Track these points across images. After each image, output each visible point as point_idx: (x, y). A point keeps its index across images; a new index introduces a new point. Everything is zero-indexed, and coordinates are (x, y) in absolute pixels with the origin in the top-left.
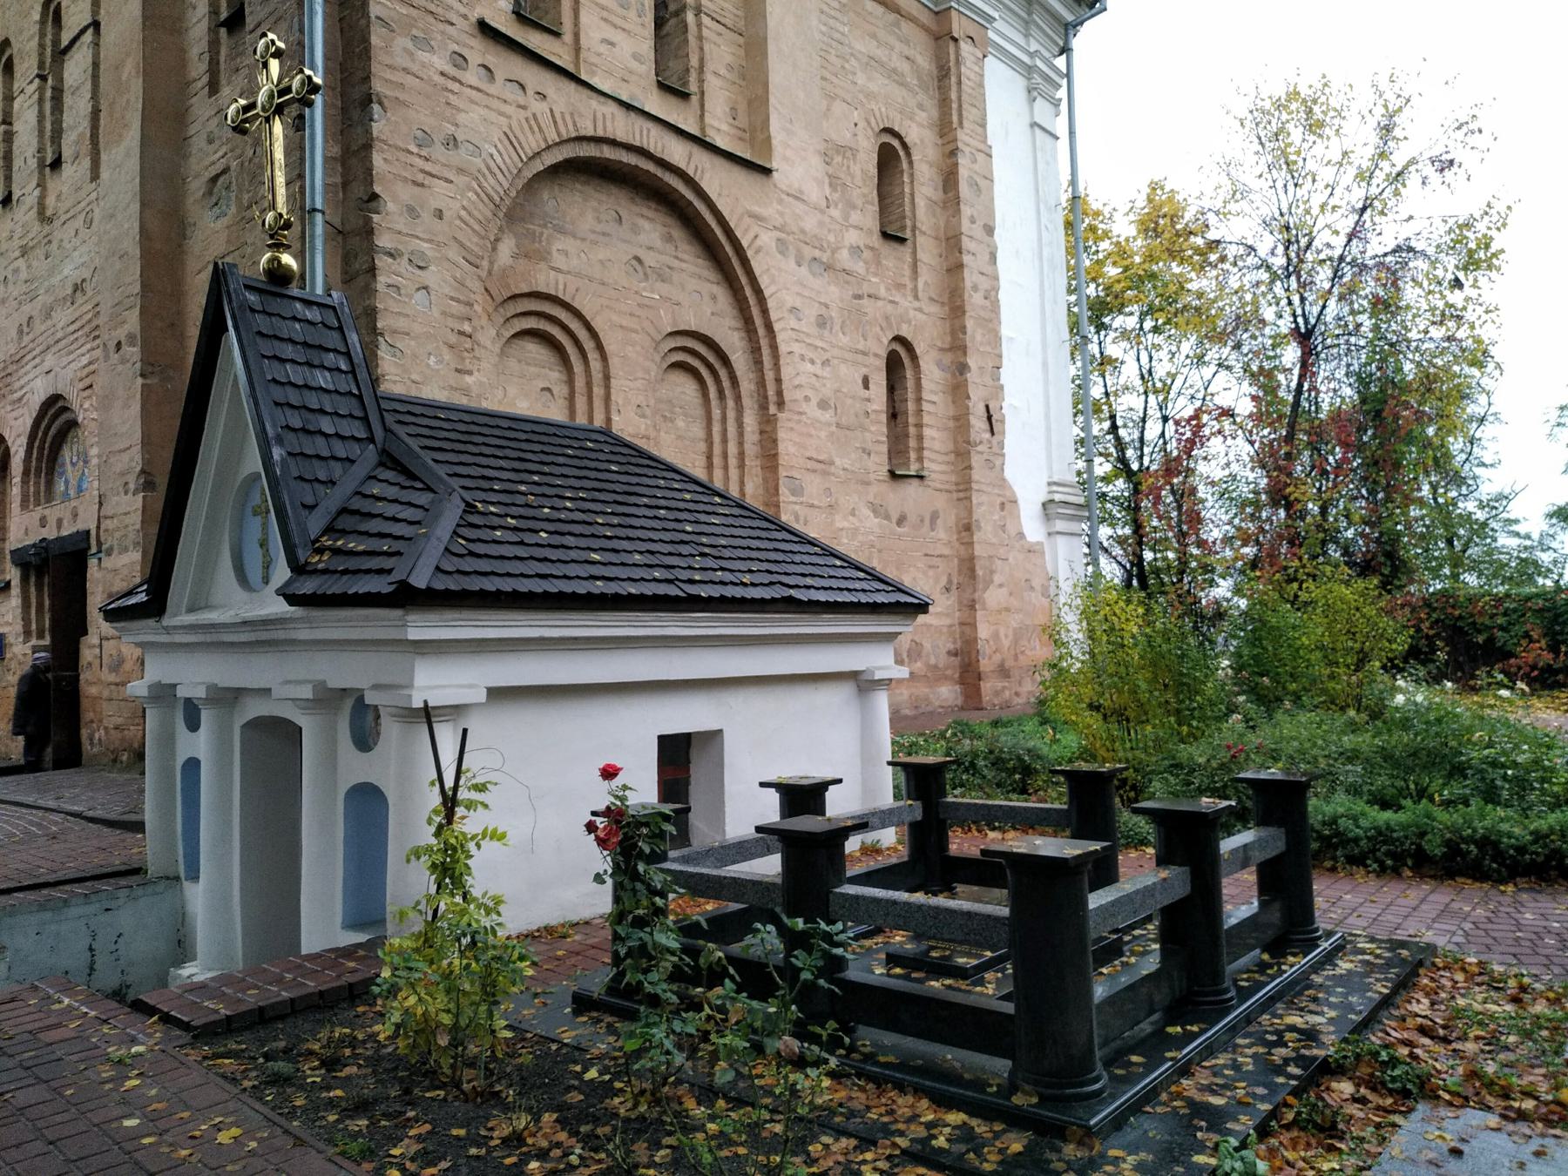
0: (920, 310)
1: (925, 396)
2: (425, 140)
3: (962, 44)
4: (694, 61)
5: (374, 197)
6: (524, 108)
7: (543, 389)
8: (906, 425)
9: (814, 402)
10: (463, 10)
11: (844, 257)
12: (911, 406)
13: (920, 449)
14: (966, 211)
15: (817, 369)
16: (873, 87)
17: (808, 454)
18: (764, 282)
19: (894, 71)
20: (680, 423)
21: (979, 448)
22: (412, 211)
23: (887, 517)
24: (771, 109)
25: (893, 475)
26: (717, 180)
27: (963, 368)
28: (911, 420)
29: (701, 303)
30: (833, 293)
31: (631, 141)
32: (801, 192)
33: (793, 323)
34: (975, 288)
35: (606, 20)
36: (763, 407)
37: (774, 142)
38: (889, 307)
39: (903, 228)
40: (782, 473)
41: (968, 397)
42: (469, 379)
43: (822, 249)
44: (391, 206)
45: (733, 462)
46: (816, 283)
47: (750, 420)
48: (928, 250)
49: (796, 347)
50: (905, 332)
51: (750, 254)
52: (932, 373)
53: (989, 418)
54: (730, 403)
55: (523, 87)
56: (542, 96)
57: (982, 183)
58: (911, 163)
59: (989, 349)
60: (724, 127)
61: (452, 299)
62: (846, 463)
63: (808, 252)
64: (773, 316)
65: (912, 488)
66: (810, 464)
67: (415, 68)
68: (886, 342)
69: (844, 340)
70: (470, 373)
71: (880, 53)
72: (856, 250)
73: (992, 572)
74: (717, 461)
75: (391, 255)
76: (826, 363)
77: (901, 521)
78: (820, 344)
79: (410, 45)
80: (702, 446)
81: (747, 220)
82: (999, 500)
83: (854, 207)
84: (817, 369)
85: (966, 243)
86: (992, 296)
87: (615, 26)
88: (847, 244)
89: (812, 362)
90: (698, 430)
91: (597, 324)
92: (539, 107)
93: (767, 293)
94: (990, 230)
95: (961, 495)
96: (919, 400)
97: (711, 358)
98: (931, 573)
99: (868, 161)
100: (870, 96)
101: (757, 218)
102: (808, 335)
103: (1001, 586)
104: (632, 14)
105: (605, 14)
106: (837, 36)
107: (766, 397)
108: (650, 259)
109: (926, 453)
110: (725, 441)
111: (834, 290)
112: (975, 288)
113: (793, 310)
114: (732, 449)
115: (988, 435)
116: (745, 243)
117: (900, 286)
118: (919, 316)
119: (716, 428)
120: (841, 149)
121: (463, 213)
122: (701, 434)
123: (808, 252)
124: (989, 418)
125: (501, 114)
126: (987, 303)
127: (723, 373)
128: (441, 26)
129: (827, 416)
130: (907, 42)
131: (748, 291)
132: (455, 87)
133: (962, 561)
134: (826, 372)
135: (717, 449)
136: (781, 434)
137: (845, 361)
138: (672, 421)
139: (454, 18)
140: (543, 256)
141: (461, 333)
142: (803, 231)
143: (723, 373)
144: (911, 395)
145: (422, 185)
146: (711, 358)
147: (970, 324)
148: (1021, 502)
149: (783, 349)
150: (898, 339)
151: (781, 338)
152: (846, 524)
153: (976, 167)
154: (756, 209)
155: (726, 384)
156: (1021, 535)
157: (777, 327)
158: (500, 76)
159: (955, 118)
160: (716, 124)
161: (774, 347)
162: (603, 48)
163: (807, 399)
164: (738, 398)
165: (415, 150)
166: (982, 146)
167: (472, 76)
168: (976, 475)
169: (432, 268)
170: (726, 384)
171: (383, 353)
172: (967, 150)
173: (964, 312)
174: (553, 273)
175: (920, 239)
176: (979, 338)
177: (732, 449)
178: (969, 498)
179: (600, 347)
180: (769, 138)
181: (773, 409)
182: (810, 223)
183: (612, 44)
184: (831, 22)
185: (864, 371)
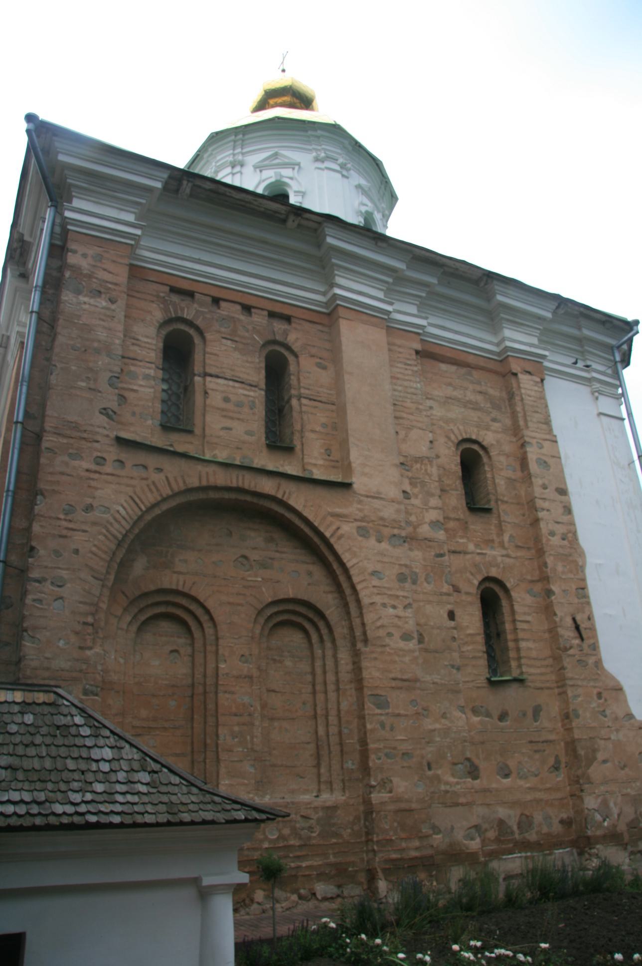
0: (508, 556)
1: (518, 617)
2: (70, 510)
3: (520, 376)
4: (298, 427)
5: (32, 549)
6: (146, 479)
7: (172, 651)
8: (506, 640)
9: (397, 634)
10: (105, 432)
11: (425, 530)
12: (508, 626)
13: (519, 658)
14: (537, 482)
15: (400, 612)
16: (451, 415)
17: (392, 675)
18: (345, 557)
19: (470, 402)
20: (288, 663)
21: (571, 652)
22: (57, 553)
23: (488, 715)
24: (351, 445)
25: (491, 683)
26: (300, 500)
27: (549, 593)
28: (510, 637)
30: (417, 557)
31: (229, 484)
32: (379, 493)
33: (375, 582)
34: (552, 534)
35: (225, 416)
36: (354, 644)
37: (353, 465)
38: (478, 558)
39: (489, 501)
40: (367, 692)
41: (555, 614)
42: (89, 653)
43: (400, 528)
44: (42, 552)
45: (331, 687)
46: (398, 552)
47: (344, 656)
48: (510, 515)
49: (378, 599)
50: (494, 572)
51: (332, 541)
52: (522, 603)
53: (577, 628)
54: (328, 645)
55: (145, 467)
56: (160, 470)
57: (551, 461)
58: (490, 457)
59: (571, 576)
60: (321, 462)
61: (81, 602)
62: (436, 678)
63: (387, 531)
64: (355, 579)
65: (512, 692)
66: (394, 684)
68: (476, 582)
69: (428, 587)
71: (457, 394)
72: (434, 524)
73: (595, 751)
74: (319, 687)
75: (39, 581)
76: (405, 607)
77: (503, 717)
78: (401, 593)
79: (66, 458)
80: (309, 678)
81: (330, 519)
82: (595, 691)
83: (432, 495)
84: (400, 612)
85: (539, 503)
86: (571, 537)
88: (427, 520)
89: (394, 607)
90: (305, 667)
91: (210, 604)
93: (349, 565)
94: (563, 492)
95: (560, 690)
96: (514, 621)
97: (311, 615)
98: (537, 756)
99: (452, 461)
100: (448, 421)
102: (389, 589)
103: (605, 762)
105: (225, 413)
106: (410, 390)
107: (354, 637)
108: (254, 556)
109: (523, 661)
110: (325, 672)
111: (417, 554)
112: (552, 534)
113: (374, 573)
114: (331, 677)
115: (577, 641)
116: (328, 534)
117: (489, 542)
118: (507, 560)
120: (419, 460)
121: (94, 549)
122: (308, 669)
123: (387, 531)
124: (577, 628)
125: (128, 485)
126: (565, 543)
127: (321, 625)
128: (89, 445)
129: (412, 645)
130: (479, 383)
131: (335, 566)
132: (96, 476)
133: (567, 744)
134: (409, 613)
135: (319, 678)
136: (365, 664)
137: (430, 602)
138: (281, 662)
139: (99, 438)
141: (85, 623)
142: (382, 519)
143: (321, 625)
144: (507, 618)
145: (65, 537)
146: (311, 615)
147: (550, 560)
148: (626, 689)
149: (365, 601)
150: (488, 579)
151: (362, 594)
152: (438, 726)
153: (544, 451)
154: (338, 510)
155: (324, 631)
156: (630, 716)
157: (359, 587)
158: (129, 464)
159: (521, 423)
160: (313, 461)
161: (358, 601)
162: (222, 433)
163: (389, 635)
164: (333, 641)
165: (62, 516)
166: (548, 437)
167: (108, 468)
168: (569, 674)
169: (69, 585)
170: (324, 631)
171: (27, 644)
172: (534, 441)
173: (544, 553)
174: (175, 576)
175: (502, 507)
176: (560, 568)
177: (331, 677)
178: (565, 693)
179: (212, 619)
180: (350, 464)
181: (360, 645)
182: (389, 512)
183: (230, 429)
184: (406, 383)
185: (449, 607)
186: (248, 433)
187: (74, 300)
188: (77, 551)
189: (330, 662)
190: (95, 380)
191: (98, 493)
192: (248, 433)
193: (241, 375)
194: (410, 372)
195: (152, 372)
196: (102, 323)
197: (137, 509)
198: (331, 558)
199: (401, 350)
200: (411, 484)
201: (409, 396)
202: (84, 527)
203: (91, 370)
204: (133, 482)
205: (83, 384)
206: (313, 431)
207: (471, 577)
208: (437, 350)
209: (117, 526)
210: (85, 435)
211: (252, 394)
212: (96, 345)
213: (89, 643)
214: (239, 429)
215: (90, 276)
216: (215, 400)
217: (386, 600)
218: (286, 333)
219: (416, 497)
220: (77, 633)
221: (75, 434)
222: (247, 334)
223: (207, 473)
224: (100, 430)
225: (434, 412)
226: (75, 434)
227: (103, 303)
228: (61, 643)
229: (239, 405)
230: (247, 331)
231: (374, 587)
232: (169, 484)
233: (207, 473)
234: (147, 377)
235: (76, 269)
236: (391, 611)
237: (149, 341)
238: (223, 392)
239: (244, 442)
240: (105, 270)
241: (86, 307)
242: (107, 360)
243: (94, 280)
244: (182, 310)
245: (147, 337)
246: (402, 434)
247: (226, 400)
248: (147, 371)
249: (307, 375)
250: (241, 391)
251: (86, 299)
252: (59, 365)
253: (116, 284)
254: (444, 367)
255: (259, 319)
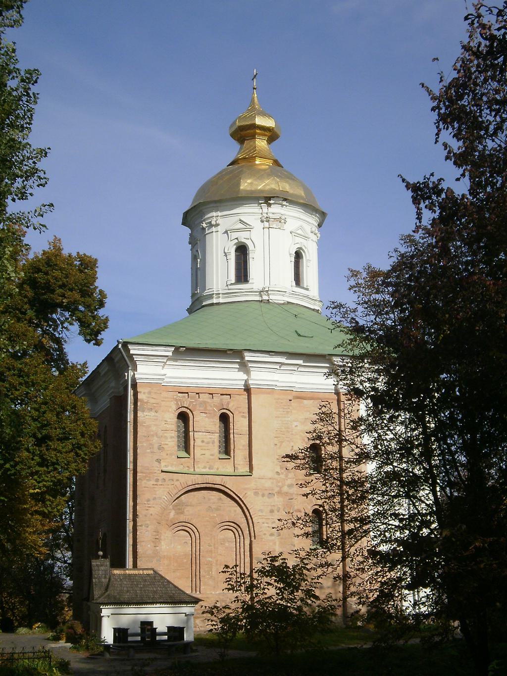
20: (227, 544)
29: (233, 512)
32: (264, 476)
35: (202, 449)
42: (157, 548)
55: (173, 480)
67: (147, 486)
70: (158, 547)
78: (270, 517)
87: (205, 450)
88: (286, 484)
89: (267, 523)
92: (177, 483)
101: (245, 489)
104: (211, 444)
106: (284, 422)
108: (213, 506)
114: (242, 550)
119: (238, 545)
123: (266, 493)
125: (167, 488)
138: (224, 544)
140: (182, 513)
154: (246, 486)
158: (167, 480)
163: (265, 534)
165: (146, 503)
167: (160, 483)
170: (240, 532)
174: (185, 517)
182: (268, 484)
186: (212, 455)
187: (143, 415)
188: (151, 515)
189: (242, 545)
190: (153, 448)
191: (157, 492)
192: (212, 455)
193: (209, 429)
194: (285, 412)
195: (173, 435)
196: (153, 423)
197: (170, 497)
198: (243, 505)
199: (282, 401)
200: (281, 468)
201: (284, 425)
202: (154, 506)
203: (151, 444)
204: (169, 486)
205: (149, 451)
206: (239, 449)
207: (308, 505)
208: (303, 395)
209: (164, 503)
210: (151, 471)
211: (213, 437)
212: (152, 433)
213: (157, 545)
214: (208, 453)
215: (147, 403)
216: (198, 442)
217: (264, 520)
218: (228, 404)
219: (282, 473)
220: (153, 542)
221: (148, 471)
222: (211, 409)
223: (195, 479)
224: (156, 468)
225: (298, 428)
226: (148, 471)
227: (153, 414)
228: (149, 546)
229: (208, 443)
230: (211, 407)
231: (259, 516)
232: (181, 485)
233: (195, 479)
234: (172, 437)
235: (142, 401)
236: (266, 525)
237: (171, 420)
238: (202, 438)
239: (210, 459)
240: (153, 398)
241: (147, 417)
242: (156, 439)
243: (149, 404)
244: (184, 402)
245: (170, 419)
246: (279, 444)
247: (203, 441)
248: (171, 435)
249: (239, 424)
250: (209, 437)
251: (147, 414)
252: (140, 445)
253: (157, 404)
254: (305, 402)
255: (217, 399)
